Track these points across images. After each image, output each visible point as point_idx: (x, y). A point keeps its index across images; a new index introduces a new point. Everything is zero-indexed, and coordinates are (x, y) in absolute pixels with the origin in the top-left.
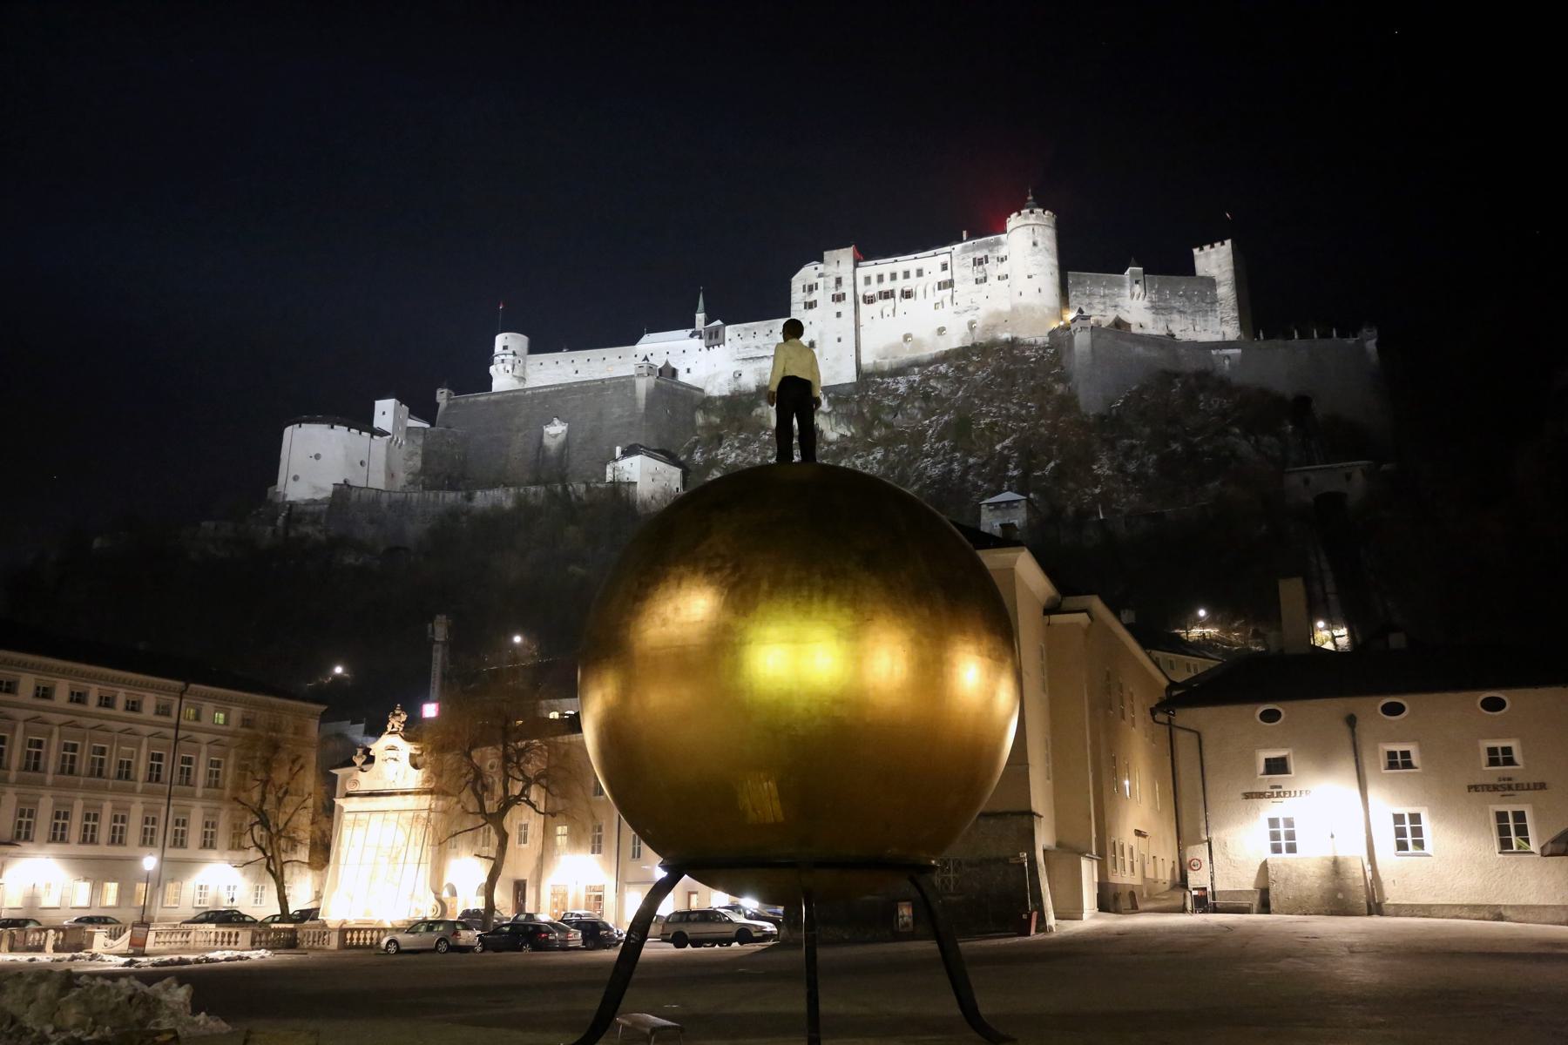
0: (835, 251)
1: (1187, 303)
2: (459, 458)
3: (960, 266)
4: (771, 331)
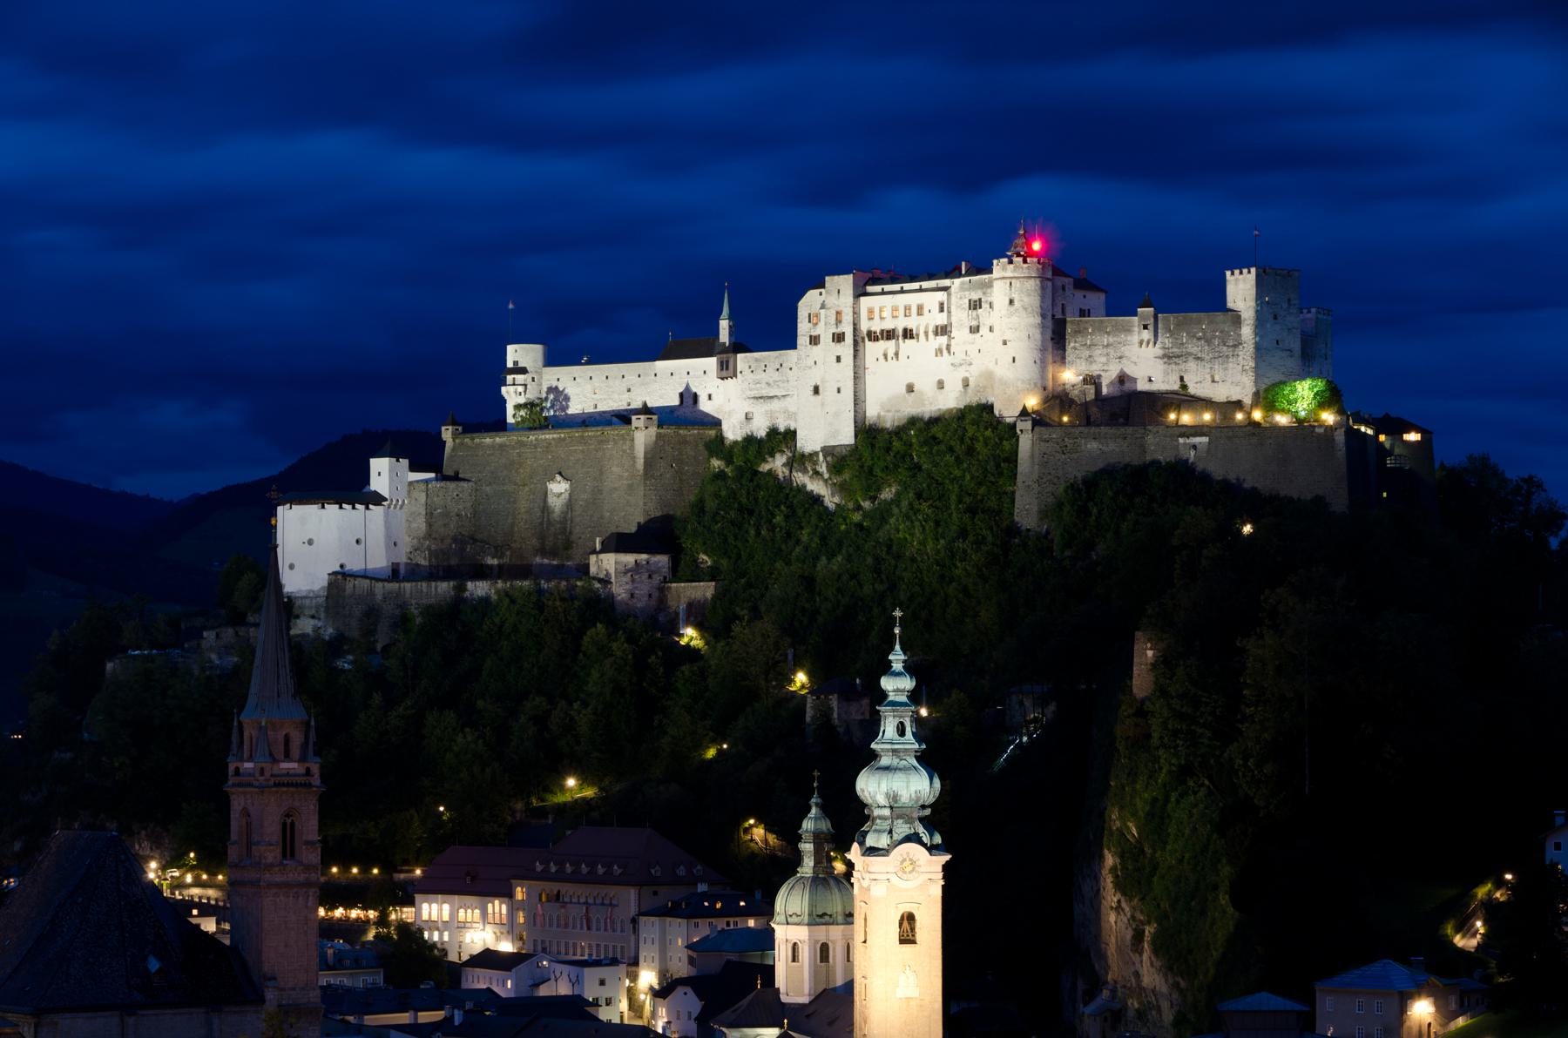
0: (836, 277)
1: (1206, 347)
2: (466, 515)
3: (958, 307)
4: (781, 365)
